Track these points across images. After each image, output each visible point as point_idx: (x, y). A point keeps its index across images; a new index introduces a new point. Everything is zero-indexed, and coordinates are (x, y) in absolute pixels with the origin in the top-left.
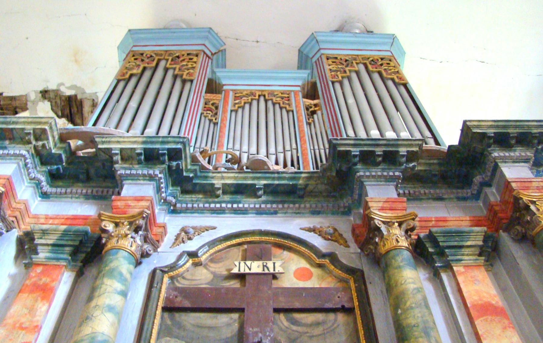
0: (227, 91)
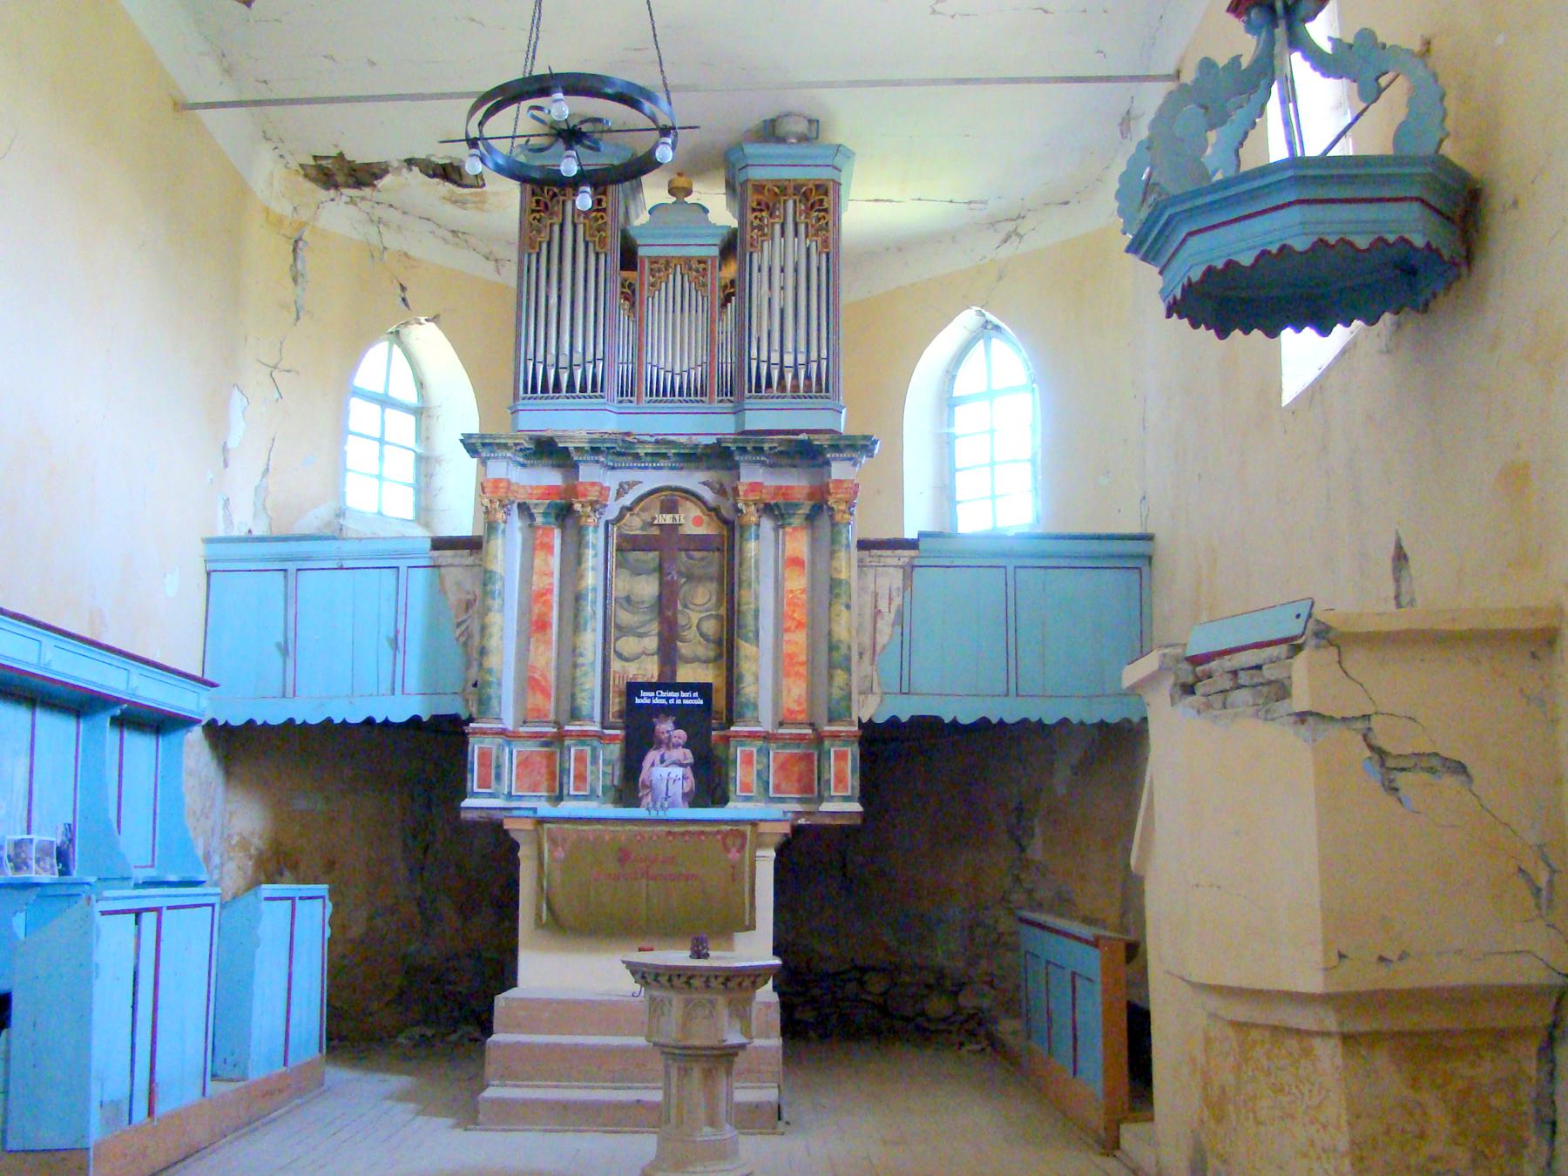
0: (642, 259)
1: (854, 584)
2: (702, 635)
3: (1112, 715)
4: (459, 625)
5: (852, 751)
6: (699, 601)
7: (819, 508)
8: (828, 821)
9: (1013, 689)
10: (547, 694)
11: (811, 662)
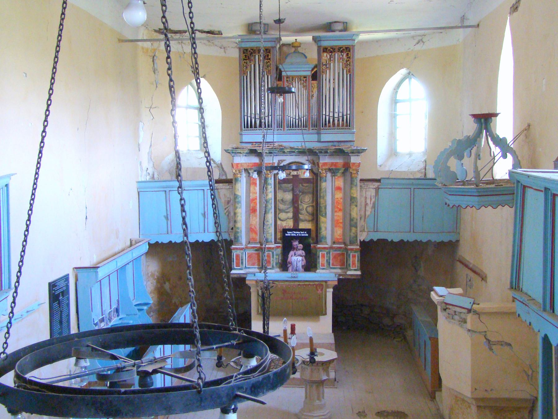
0: (284, 76)
1: (358, 197)
2: (307, 212)
3: (445, 238)
4: (225, 209)
5: (357, 254)
6: (306, 201)
7: (347, 166)
8: (349, 277)
9: (412, 230)
10: (256, 233)
11: (344, 223)
